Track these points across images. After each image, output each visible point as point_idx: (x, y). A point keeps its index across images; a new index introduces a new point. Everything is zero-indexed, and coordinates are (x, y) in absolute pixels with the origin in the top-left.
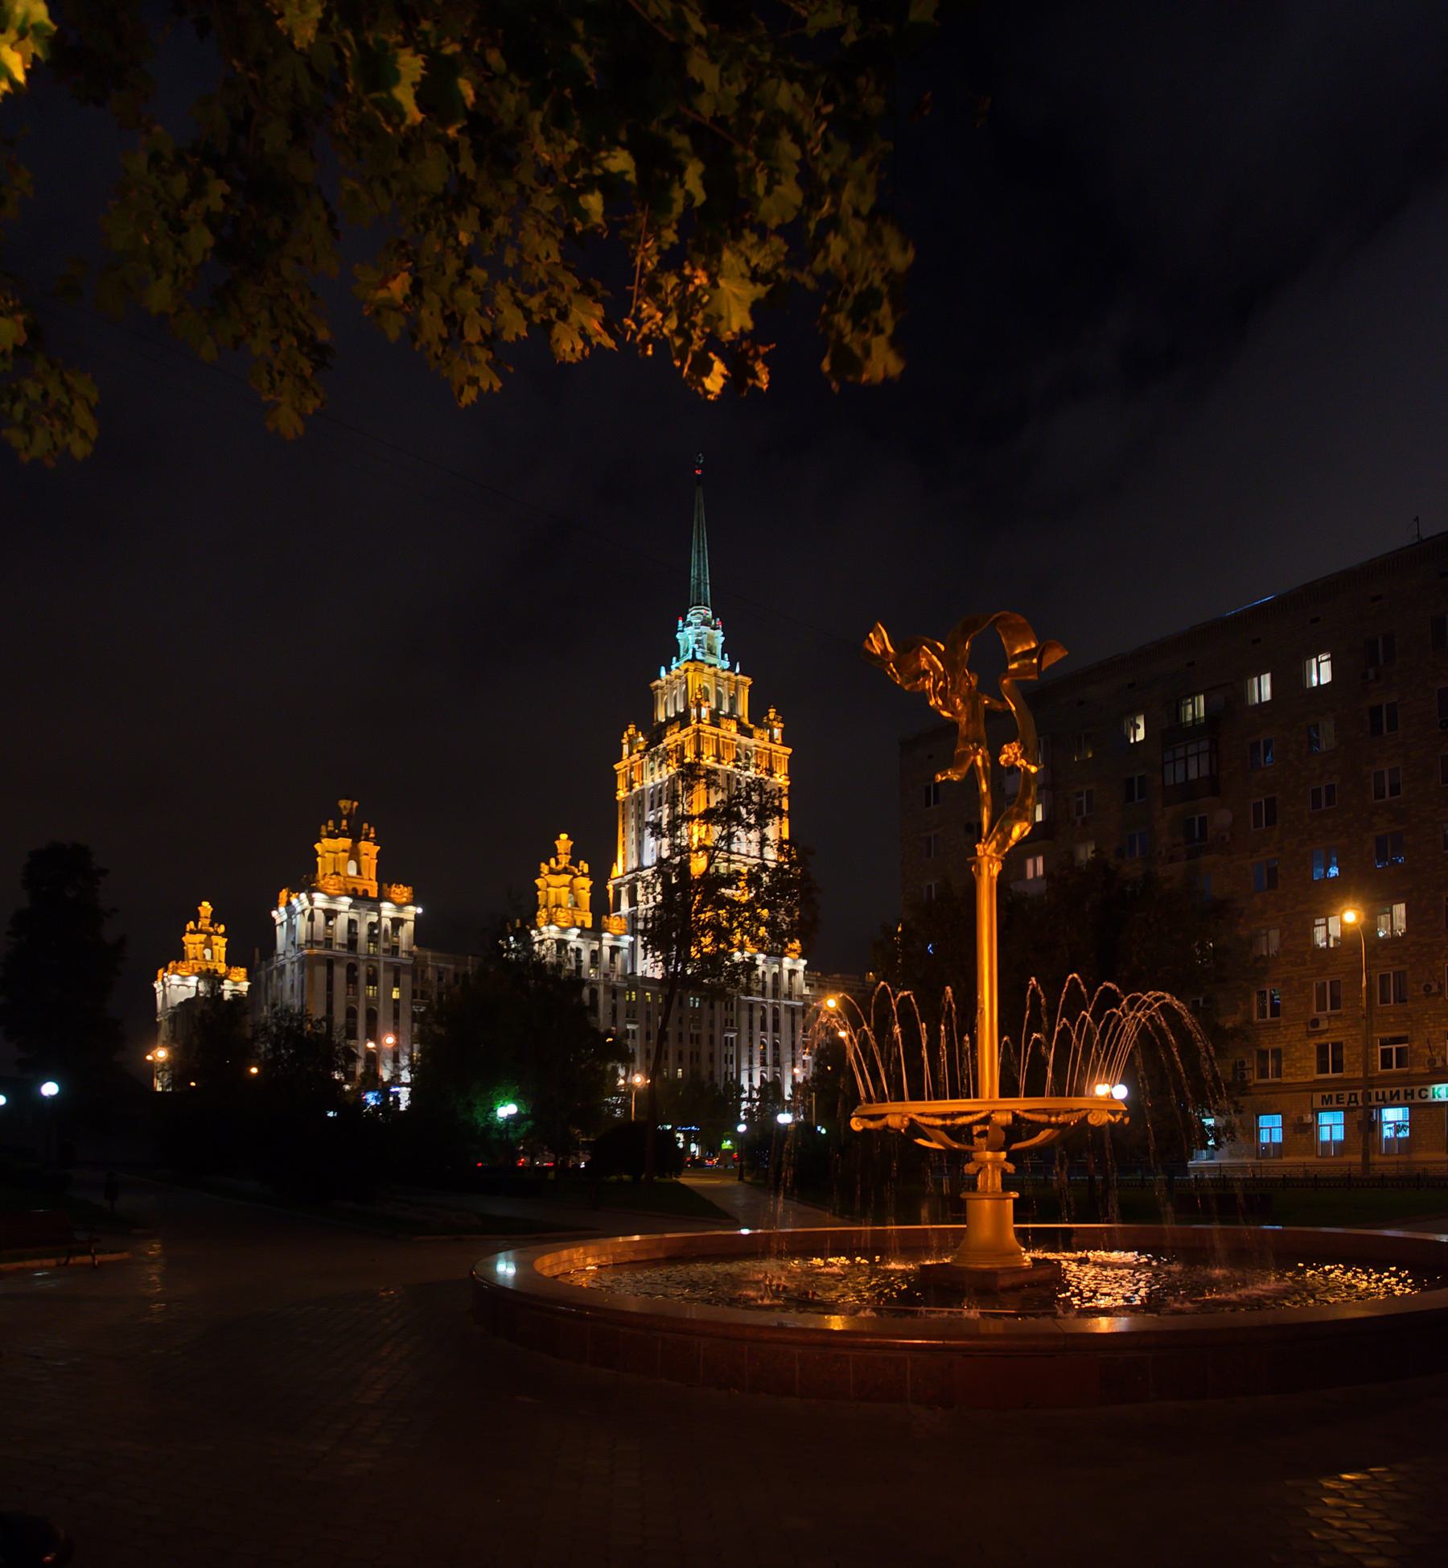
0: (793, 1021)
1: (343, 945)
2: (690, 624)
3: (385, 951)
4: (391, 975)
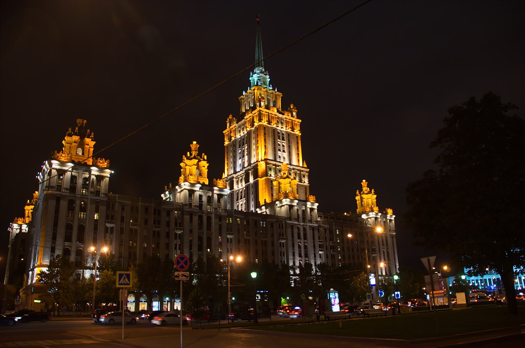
0: (313, 233)
1: (67, 189)
2: (255, 73)
3: (91, 193)
4: (94, 206)
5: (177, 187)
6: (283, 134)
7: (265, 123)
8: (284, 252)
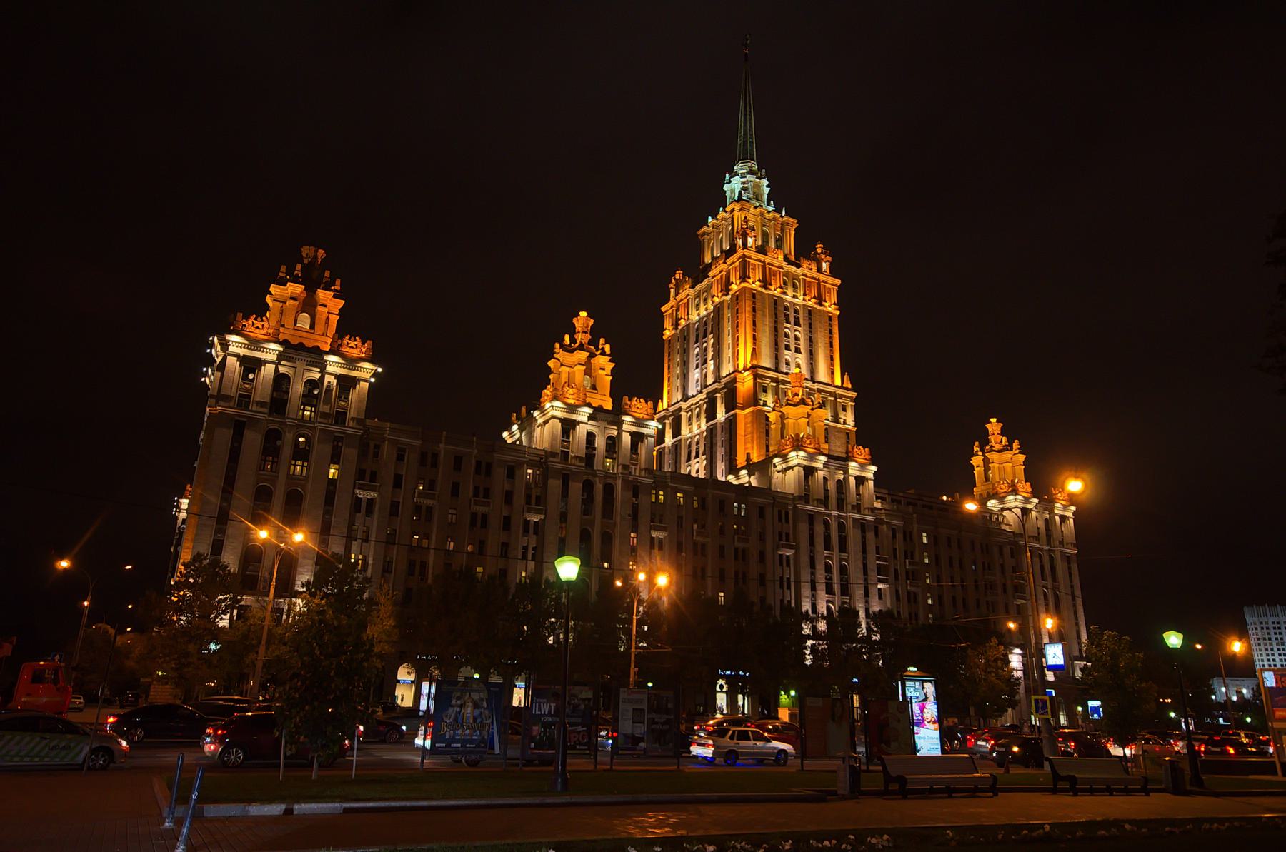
0: (864, 538)
1: (262, 404)
2: (737, 174)
3: (324, 415)
4: (328, 449)
5: (536, 413)
6: (796, 312)
7: (756, 286)
8: (788, 579)
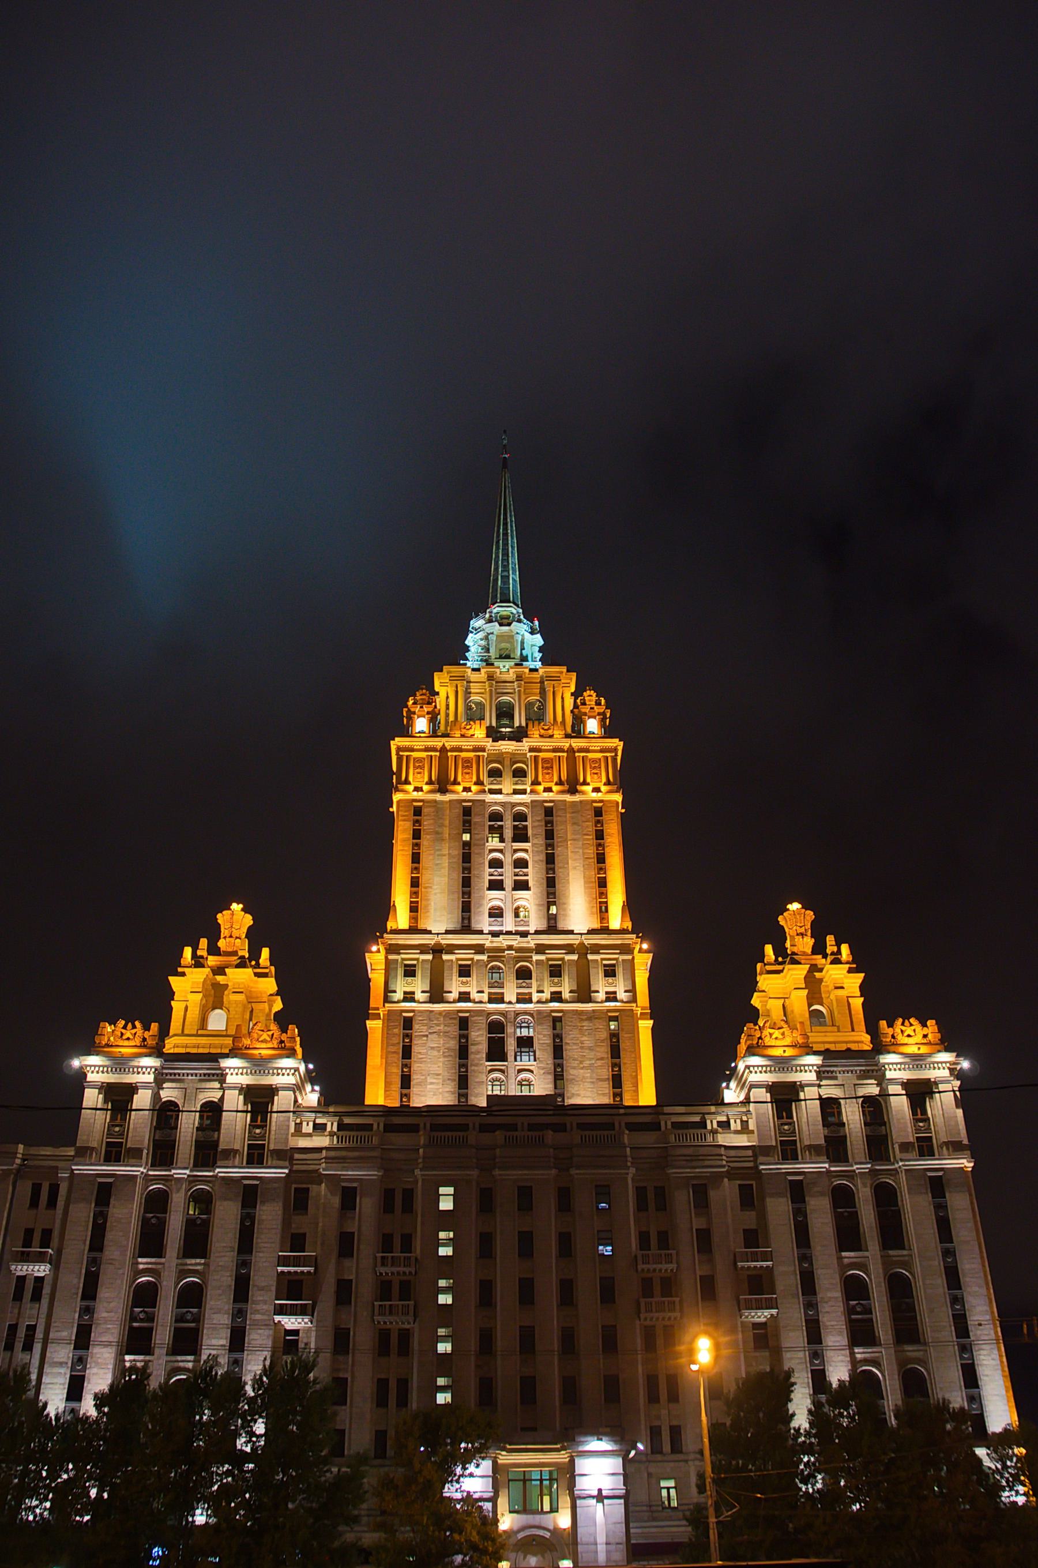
6: (520, 817)
